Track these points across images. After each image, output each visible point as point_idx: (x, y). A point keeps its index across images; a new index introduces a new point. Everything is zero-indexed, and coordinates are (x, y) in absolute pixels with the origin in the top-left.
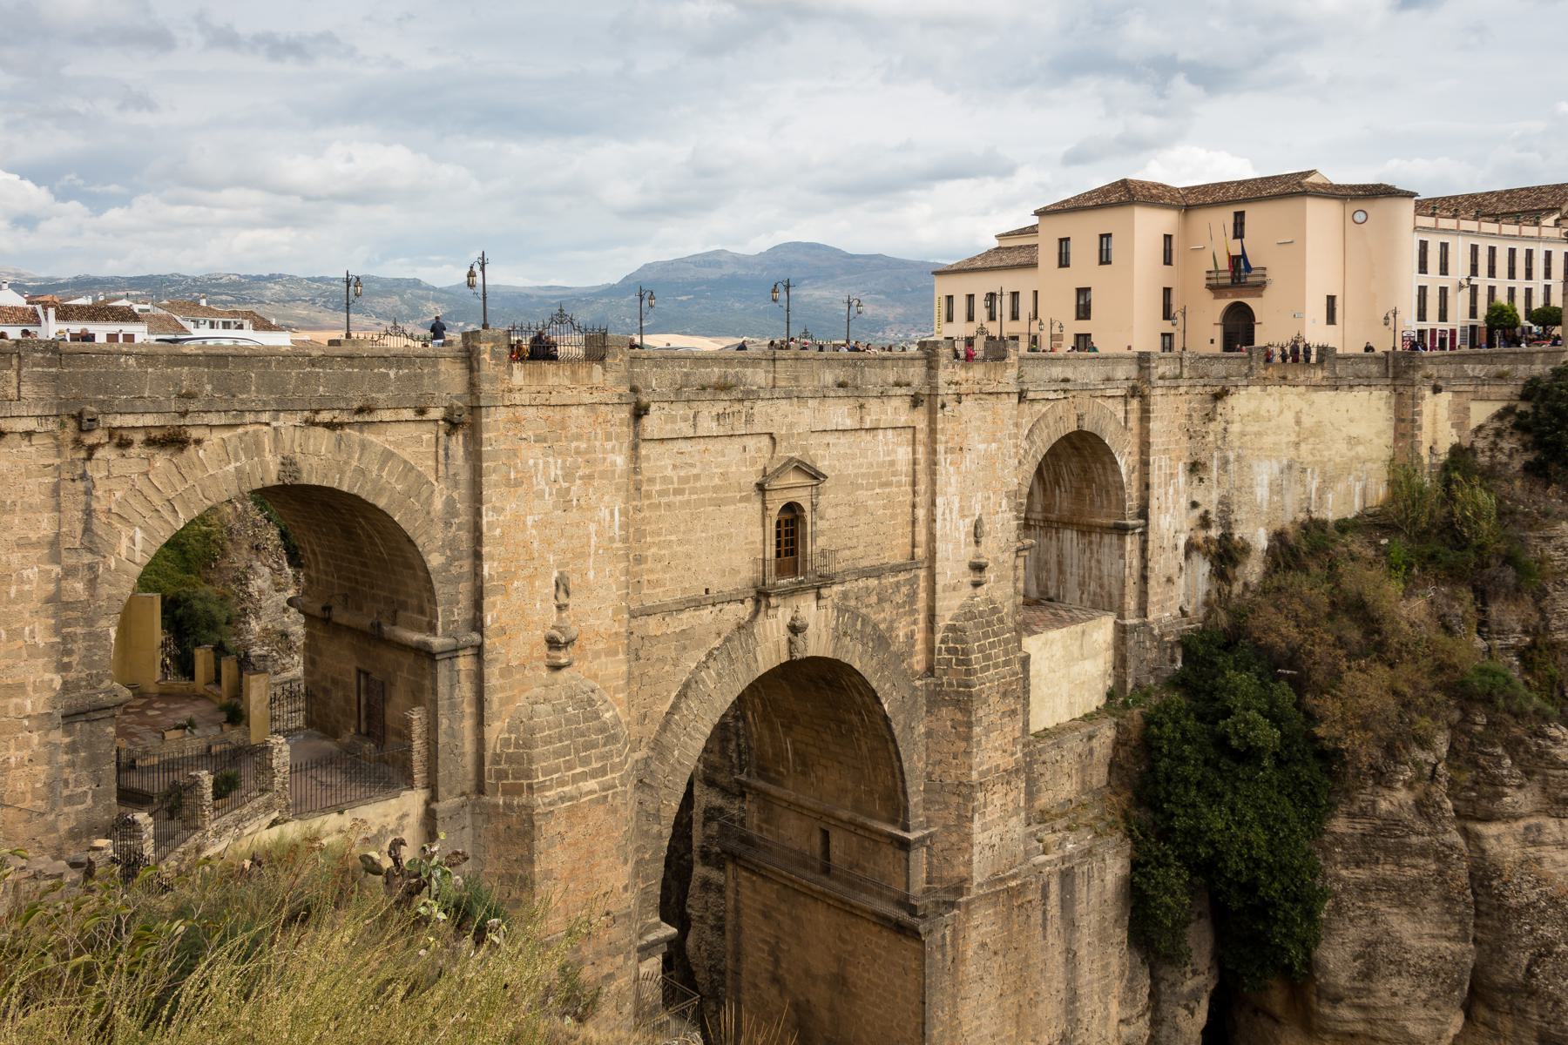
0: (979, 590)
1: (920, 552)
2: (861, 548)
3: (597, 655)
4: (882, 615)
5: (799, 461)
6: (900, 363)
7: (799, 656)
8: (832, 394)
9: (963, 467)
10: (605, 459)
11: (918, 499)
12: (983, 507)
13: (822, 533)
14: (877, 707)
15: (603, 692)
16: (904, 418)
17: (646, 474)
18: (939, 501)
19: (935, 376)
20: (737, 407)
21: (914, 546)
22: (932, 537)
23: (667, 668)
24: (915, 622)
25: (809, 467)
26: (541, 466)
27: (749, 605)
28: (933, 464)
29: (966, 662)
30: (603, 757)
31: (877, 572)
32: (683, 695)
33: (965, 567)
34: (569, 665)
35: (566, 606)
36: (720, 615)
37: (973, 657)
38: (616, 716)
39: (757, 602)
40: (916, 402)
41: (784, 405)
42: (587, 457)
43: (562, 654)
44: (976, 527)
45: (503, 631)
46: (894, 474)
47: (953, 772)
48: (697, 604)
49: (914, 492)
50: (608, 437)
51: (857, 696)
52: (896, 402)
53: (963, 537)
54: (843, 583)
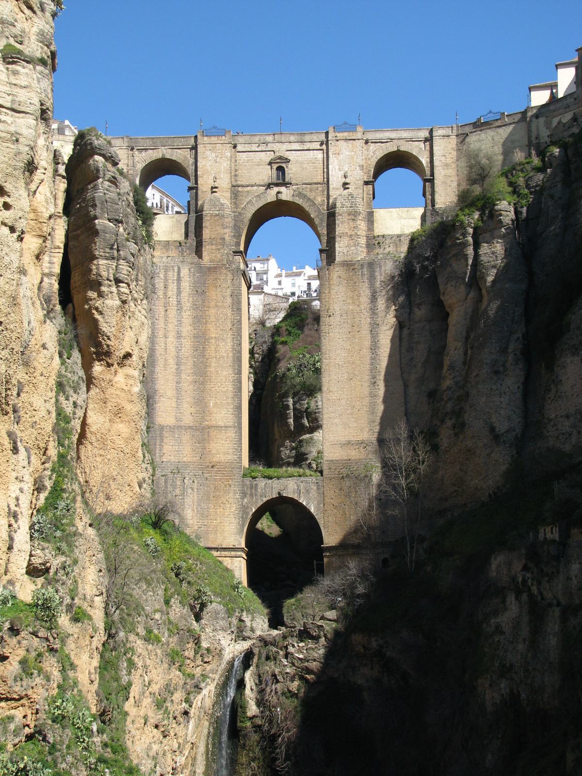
3: (223, 191)
9: (340, 158)
13: (292, 173)
16: (319, 147)
18: (330, 166)
31: (310, 184)
45: (202, 185)
53: (340, 176)
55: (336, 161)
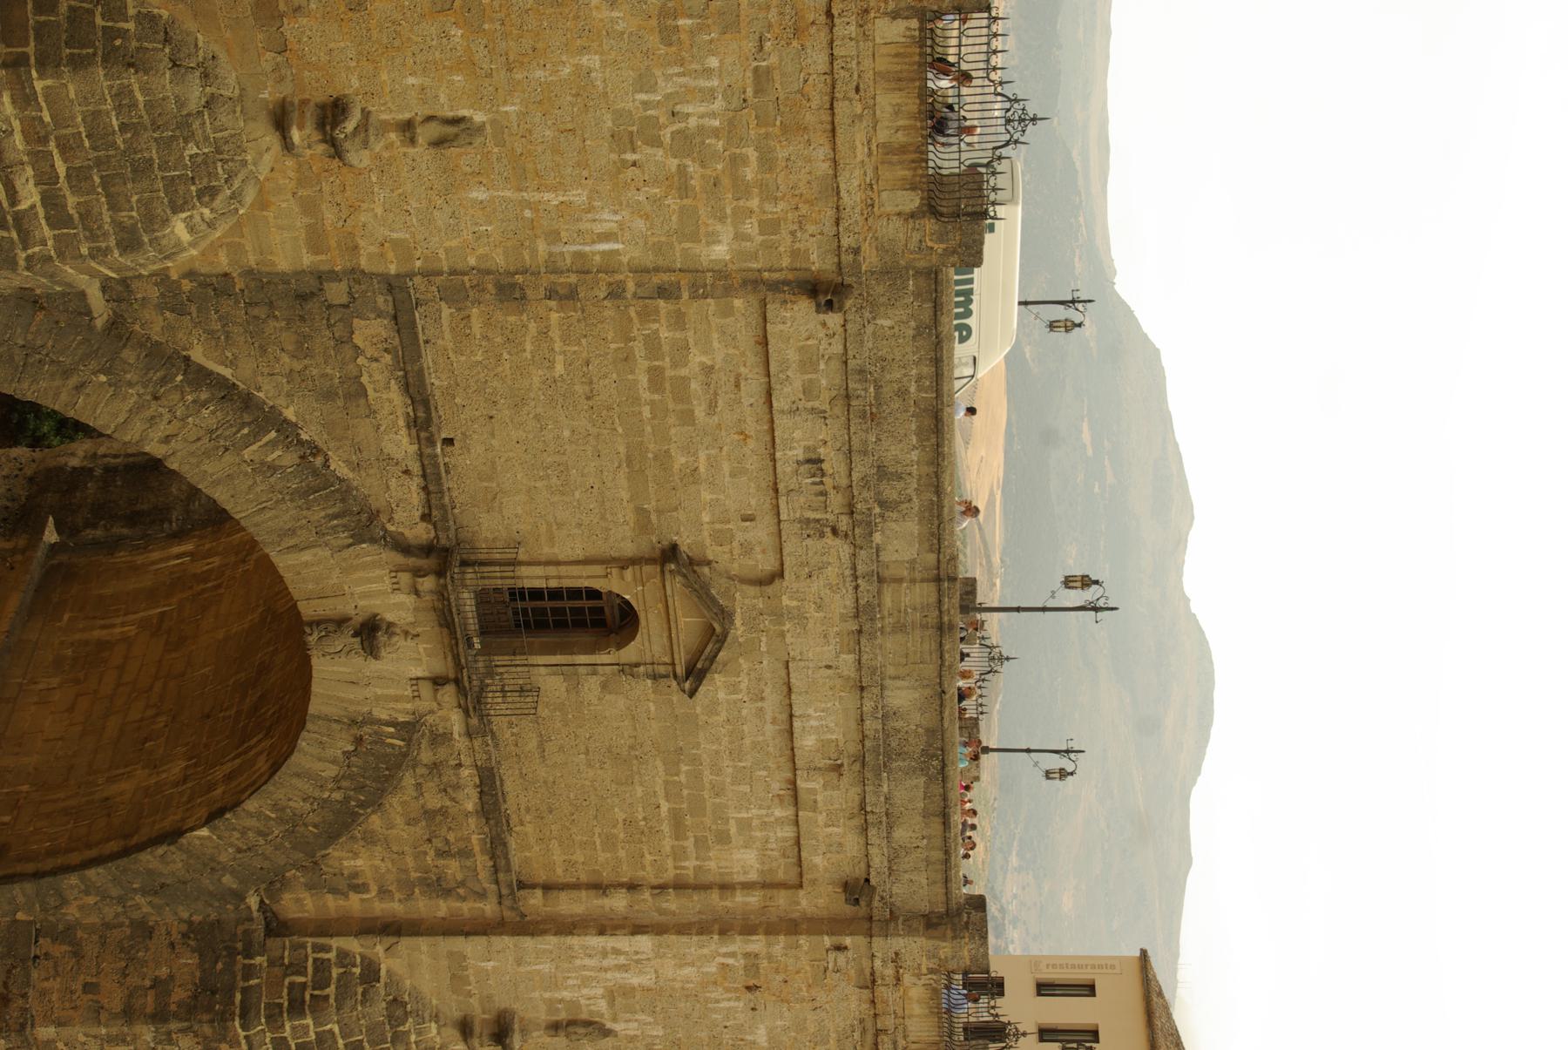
0: (452, 1033)
1: (535, 901)
2: (542, 773)
3: (309, 207)
4: (399, 820)
5: (725, 635)
6: (938, 855)
7: (312, 639)
8: (868, 706)
10: (722, 219)
11: (647, 895)
12: (632, 1039)
13: (575, 686)
14: (203, 812)
15: (232, 221)
16: (818, 860)
17: (692, 309)
18: (644, 942)
19: (911, 931)
20: (836, 501)
21: (547, 888)
22: (568, 927)
23: (286, 359)
24: (384, 893)
25: (713, 659)
26: (703, 83)
27: (420, 533)
28: (724, 927)
29: (297, 1008)
30: (86, 215)
32: (226, 392)
33: (502, 1001)
34: (287, 145)
35: (412, 141)
36: (397, 471)
37: (309, 1021)
38: (179, 247)
39: (428, 550)
40: (857, 889)
41: (842, 602)
42: (726, 181)
43: (310, 128)
44: (588, 1024)
46: (700, 843)
47: (54, 984)
48: (422, 422)
49: (662, 887)
50: (770, 226)
51: (227, 768)
52: (853, 844)
53: (566, 994)
54: (469, 734)
55: (688, 971)
